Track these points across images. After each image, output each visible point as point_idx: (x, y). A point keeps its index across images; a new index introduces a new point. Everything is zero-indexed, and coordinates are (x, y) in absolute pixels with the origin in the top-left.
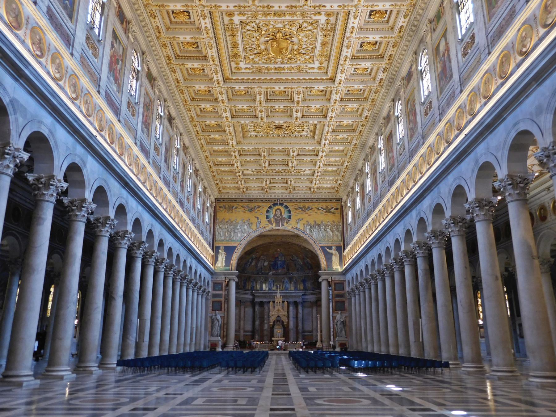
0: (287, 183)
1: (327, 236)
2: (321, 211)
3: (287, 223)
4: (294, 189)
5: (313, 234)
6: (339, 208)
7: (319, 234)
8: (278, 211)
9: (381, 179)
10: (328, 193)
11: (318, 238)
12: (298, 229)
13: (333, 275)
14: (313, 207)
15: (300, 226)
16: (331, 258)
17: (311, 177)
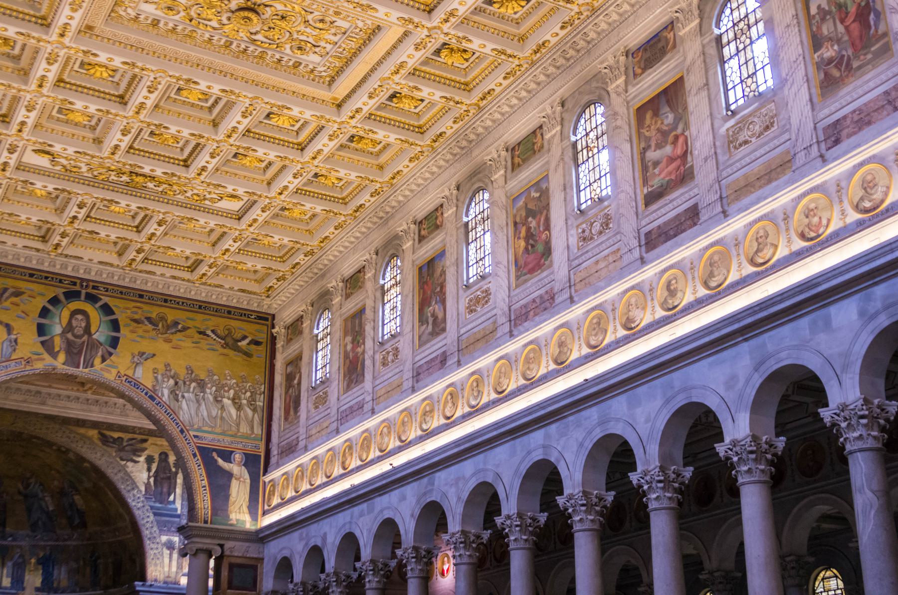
0: (139, 232)
1: (222, 418)
2: (212, 342)
3: (104, 360)
4: (145, 260)
5: (180, 408)
6: (264, 341)
7: (198, 408)
8: (80, 317)
9: (573, 232)
10: (243, 291)
11: (196, 420)
12: (137, 385)
13: (228, 539)
14: (190, 324)
15: (143, 375)
16: (228, 487)
17: (229, 223)
